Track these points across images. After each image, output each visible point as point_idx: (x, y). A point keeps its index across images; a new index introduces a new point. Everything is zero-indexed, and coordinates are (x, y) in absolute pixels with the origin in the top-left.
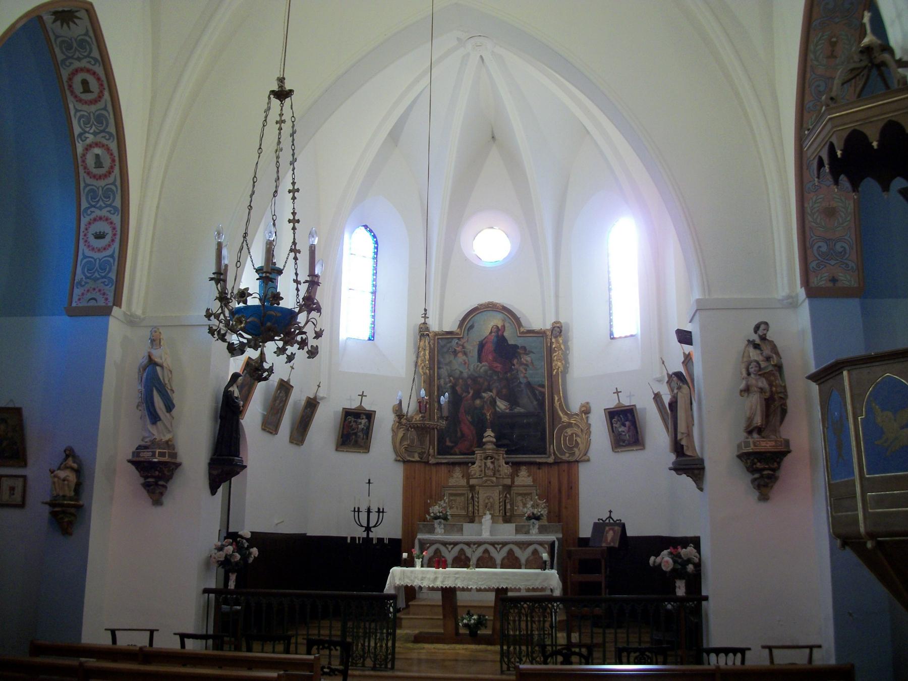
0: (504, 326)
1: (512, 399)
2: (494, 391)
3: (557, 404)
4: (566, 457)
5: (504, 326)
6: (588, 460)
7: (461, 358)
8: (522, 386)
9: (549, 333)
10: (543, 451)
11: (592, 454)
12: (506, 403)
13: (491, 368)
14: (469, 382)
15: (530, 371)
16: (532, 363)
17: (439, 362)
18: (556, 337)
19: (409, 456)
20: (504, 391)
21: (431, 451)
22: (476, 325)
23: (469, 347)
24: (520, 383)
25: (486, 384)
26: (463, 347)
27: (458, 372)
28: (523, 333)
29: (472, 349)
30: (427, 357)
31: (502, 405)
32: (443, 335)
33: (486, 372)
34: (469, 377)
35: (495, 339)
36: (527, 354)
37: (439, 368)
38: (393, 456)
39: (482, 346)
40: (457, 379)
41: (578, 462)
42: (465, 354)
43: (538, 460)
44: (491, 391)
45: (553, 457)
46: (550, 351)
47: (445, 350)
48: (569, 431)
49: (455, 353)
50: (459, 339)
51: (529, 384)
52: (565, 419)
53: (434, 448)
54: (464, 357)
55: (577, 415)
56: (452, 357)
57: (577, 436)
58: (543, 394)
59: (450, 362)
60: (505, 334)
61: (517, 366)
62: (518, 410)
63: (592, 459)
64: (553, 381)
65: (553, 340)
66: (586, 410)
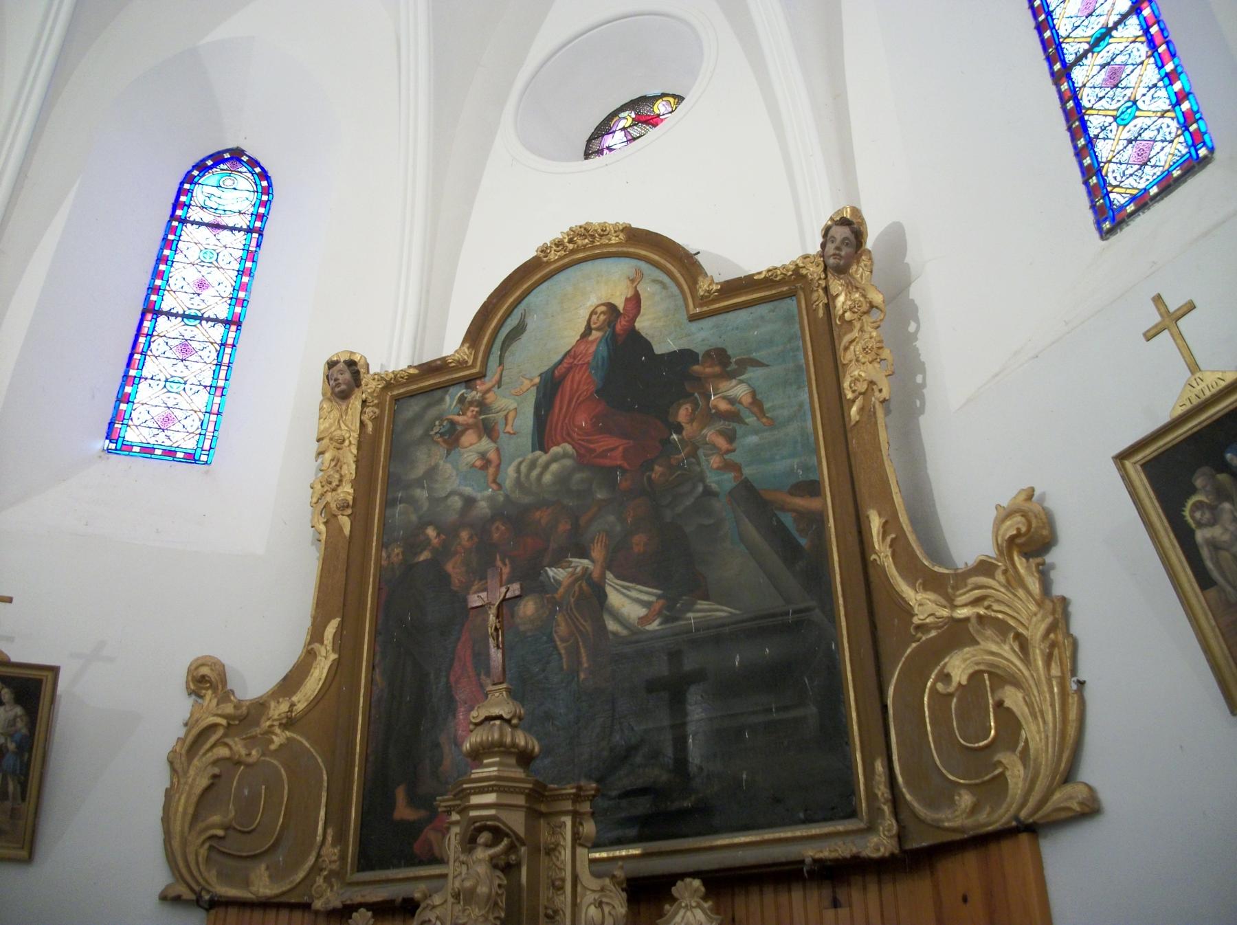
0: (635, 301)
1: (672, 566)
2: (598, 552)
3: (882, 552)
4: (960, 813)
5: (635, 301)
6: (1090, 810)
7: (473, 446)
8: (720, 505)
9: (814, 271)
10: (839, 802)
11: (1095, 771)
12: (647, 594)
13: (584, 459)
14: (498, 531)
15: (751, 437)
16: (756, 403)
17: (392, 481)
18: (841, 271)
19: (224, 877)
20: (639, 542)
21: (331, 852)
22: (532, 323)
23: (502, 402)
24: (708, 493)
25: (564, 526)
26: (483, 406)
27: (457, 502)
28: (705, 300)
29: (515, 404)
30: (350, 469)
31: (628, 604)
32: (411, 379)
33: (563, 480)
34: (498, 514)
35: (603, 350)
36: (730, 376)
37: (389, 503)
38: (158, 877)
39: (551, 387)
40: (449, 532)
41: (1030, 829)
42: (488, 430)
43: (810, 852)
44: (584, 554)
45: (889, 822)
46: (828, 333)
47: (418, 431)
48: (959, 667)
49: (452, 436)
50: (469, 382)
51: (750, 496)
52: (924, 605)
53: (340, 838)
54: (485, 444)
55: (985, 568)
56: (439, 451)
57: (1001, 678)
58: (818, 519)
59: (432, 472)
60: (643, 324)
61: (688, 430)
62: (704, 612)
63: (1106, 797)
64: (857, 447)
65: (836, 286)
66: (1031, 538)
